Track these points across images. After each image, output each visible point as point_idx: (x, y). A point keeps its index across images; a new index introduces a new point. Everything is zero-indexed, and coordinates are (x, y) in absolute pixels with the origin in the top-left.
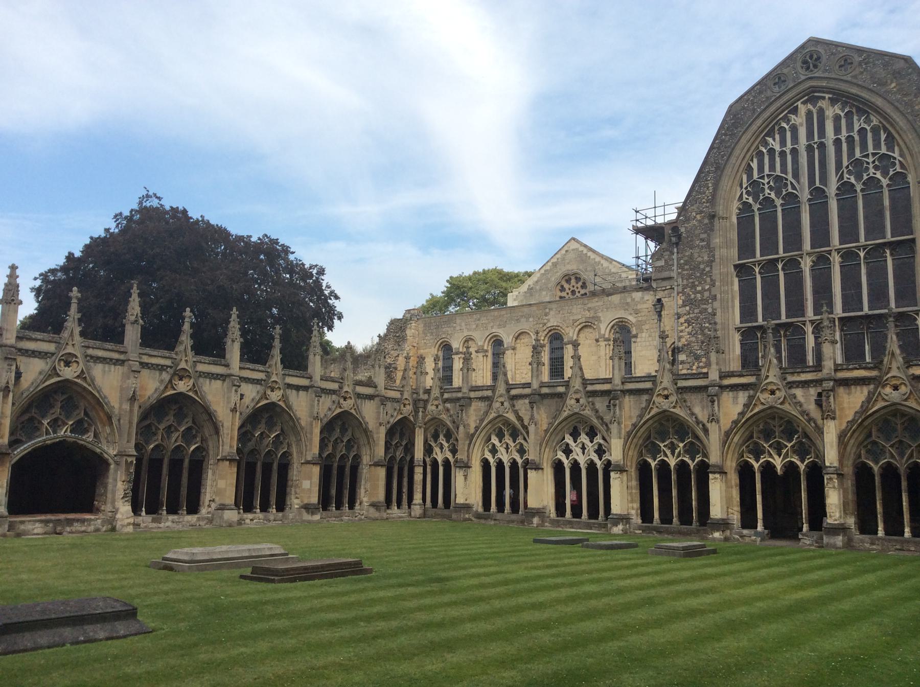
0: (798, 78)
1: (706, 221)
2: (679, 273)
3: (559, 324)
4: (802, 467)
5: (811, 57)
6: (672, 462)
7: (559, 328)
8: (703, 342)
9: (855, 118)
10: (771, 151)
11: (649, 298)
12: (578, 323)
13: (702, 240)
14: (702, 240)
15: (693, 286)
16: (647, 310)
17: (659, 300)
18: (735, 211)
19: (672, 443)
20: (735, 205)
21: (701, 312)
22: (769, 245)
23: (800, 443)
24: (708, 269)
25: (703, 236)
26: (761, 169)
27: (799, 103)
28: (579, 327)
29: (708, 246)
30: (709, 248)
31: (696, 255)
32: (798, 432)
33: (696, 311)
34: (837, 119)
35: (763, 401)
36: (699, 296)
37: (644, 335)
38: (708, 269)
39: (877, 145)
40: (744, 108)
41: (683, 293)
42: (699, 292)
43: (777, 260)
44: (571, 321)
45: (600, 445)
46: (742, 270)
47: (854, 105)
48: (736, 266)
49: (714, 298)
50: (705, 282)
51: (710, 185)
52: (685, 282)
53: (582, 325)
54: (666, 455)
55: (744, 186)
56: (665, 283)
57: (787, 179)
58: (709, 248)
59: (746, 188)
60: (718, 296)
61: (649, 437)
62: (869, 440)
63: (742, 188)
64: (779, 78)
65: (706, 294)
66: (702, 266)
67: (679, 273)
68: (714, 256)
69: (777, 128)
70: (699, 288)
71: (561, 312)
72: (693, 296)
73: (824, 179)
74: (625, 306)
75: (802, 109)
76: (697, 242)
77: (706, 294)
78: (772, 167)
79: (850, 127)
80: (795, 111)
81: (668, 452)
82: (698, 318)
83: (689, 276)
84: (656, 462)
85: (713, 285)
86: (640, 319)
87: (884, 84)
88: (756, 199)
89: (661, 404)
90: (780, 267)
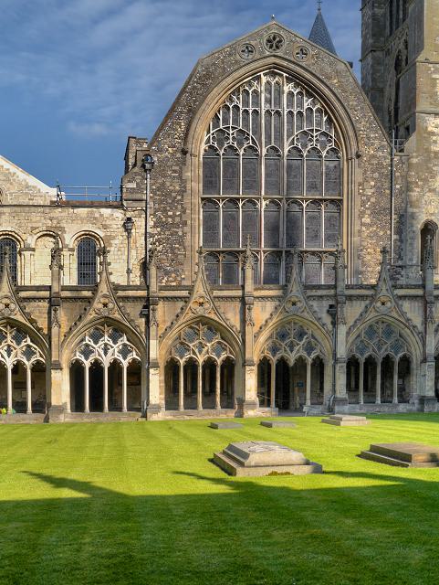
0: (263, 52)
1: (179, 155)
2: (151, 197)
3: (13, 230)
4: (310, 361)
5: (274, 38)
6: (201, 360)
7: (13, 234)
8: (173, 261)
9: (305, 98)
10: (236, 107)
11: (119, 214)
12: (37, 230)
13: (175, 171)
14: (175, 171)
15: (165, 211)
16: (115, 226)
17: (129, 219)
18: (202, 152)
19: (201, 343)
20: (204, 146)
21: (172, 235)
22: (231, 183)
23: (309, 342)
24: (179, 198)
25: (177, 168)
26: (226, 121)
27: (262, 73)
28: (39, 235)
29: (180, 177)
30: (181, 179)
31: (168, 184)
32: (306, 334)
33: (167, 233)
34: (291, 94)
35: (287, 309)
36: (170, 220)
37: (112, 249)
38: (179, 198)
39: (319, 124)
40: (214, 64)
41: (154, 215)
42: (170, 216)
43: (238, 199)
44: (29, 228)
45: (125, 345)
46: (207, 201)
47: (304, 88)
48: (203, 199)
49: (185, 224)
50: (176, 208)
51: (183, 124)
52: (157, 206)
53: (41, 234)
54: (194, 353)
55: (212, 132)
56: (135, 204)
57: (248, 135)
58: (181, 179)
59: (213, 134)
60: (189, 222)
61: (179, 337)
62: (359, 339)
63: (208, 132)
64: (247, 48)
65: (177, 219)
66: (174, 194)
67: (151, 197)
68: (185, 187)
69: (241, 90)
70: (170, 213)
71: (16, 218)
72: (164, 219)
73: (280, 138)
74: (94, 220)
75: (264, 79)
76: (169, 173)
77: (177, 219)
78: (236, 121)
79: (301, 104)
80: (259, 78)
81: (197, 351)
82: (168, 239)
83: (161, 202)
84: (184, 359)
85: (184, 212)
86: (109, 234)
87: (330, 78)
88: (221, 145)
89: (194, 309)
90: (240, 205)
